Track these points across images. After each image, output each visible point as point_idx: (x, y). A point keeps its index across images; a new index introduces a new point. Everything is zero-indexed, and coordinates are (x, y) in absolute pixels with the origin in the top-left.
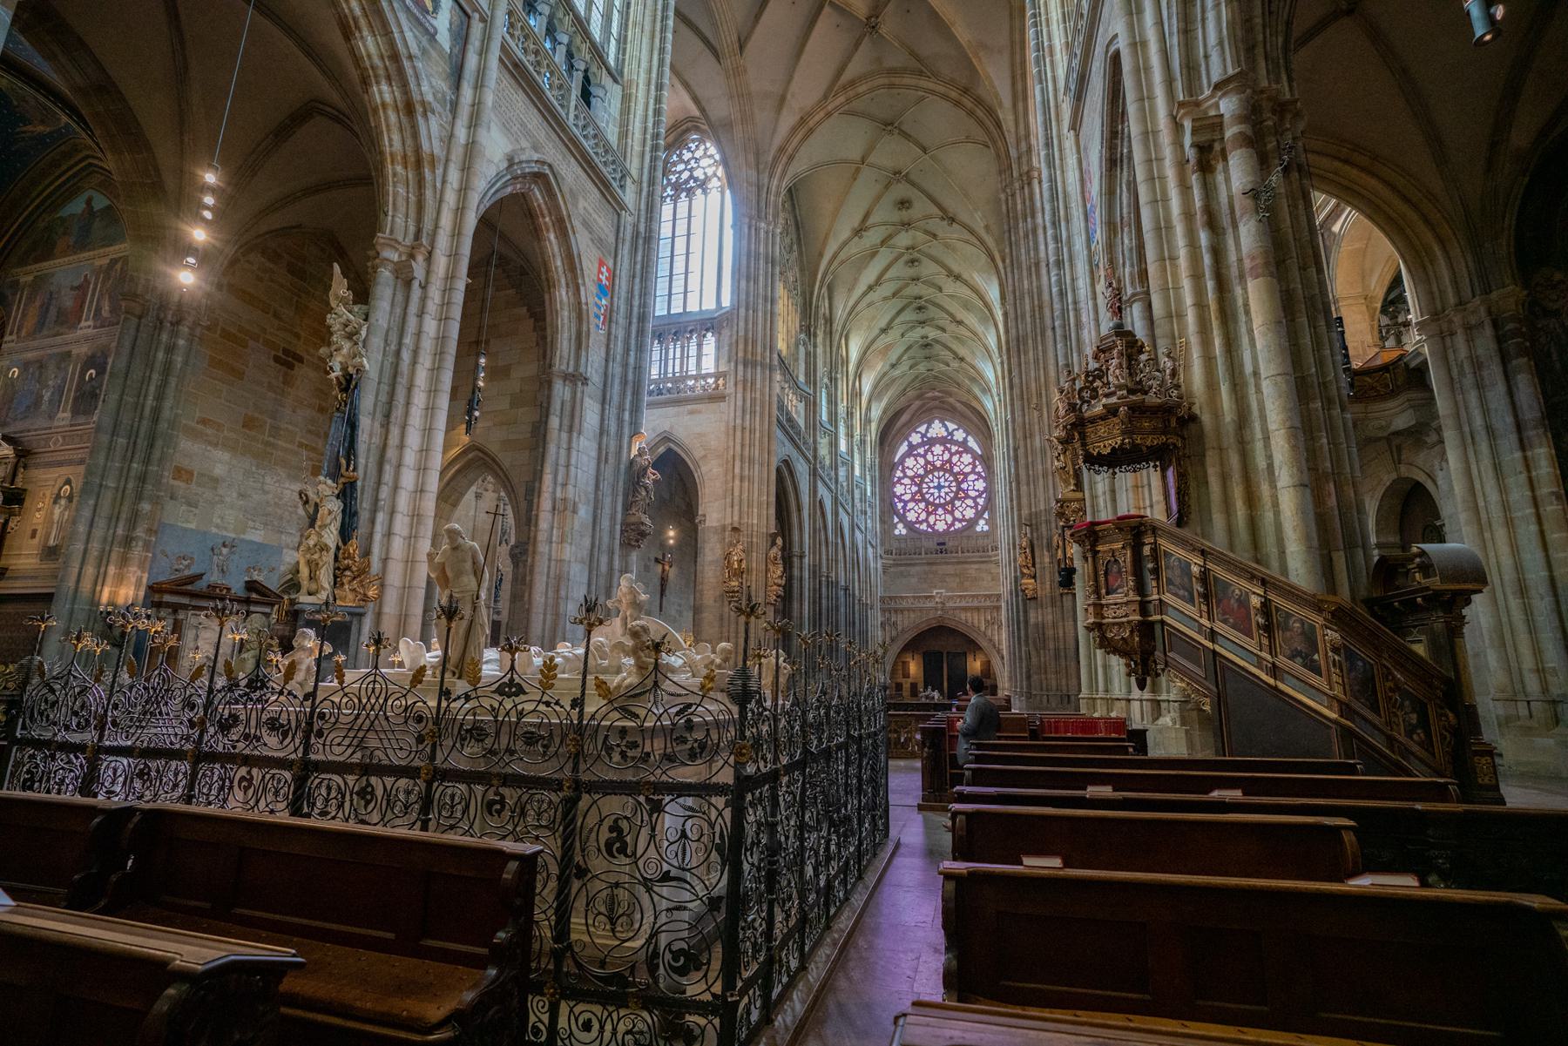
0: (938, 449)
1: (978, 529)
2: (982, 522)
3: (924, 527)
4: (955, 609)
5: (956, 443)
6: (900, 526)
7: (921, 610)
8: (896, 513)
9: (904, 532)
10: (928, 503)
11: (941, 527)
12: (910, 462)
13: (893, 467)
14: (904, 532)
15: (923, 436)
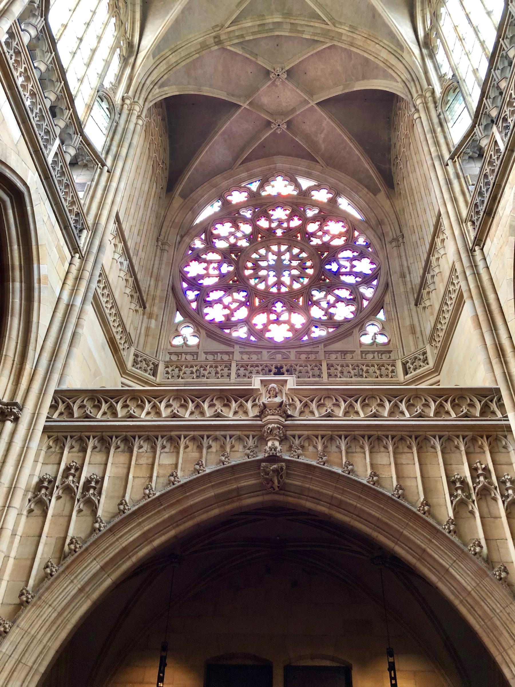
0: (280, 214)
1: (366, 340)
2: (372, 329)
3: (241, 333)
4: (331, 435)
5: (315, 204)
6: (187, 331)
7: (199, 435)
8: (181, 307)
9: (193, 341)
10: (252, 292)
11: (279, 333)
12: (224, 229)
13: (187, 231)
14: (193, 341)
15: (253, 196)
